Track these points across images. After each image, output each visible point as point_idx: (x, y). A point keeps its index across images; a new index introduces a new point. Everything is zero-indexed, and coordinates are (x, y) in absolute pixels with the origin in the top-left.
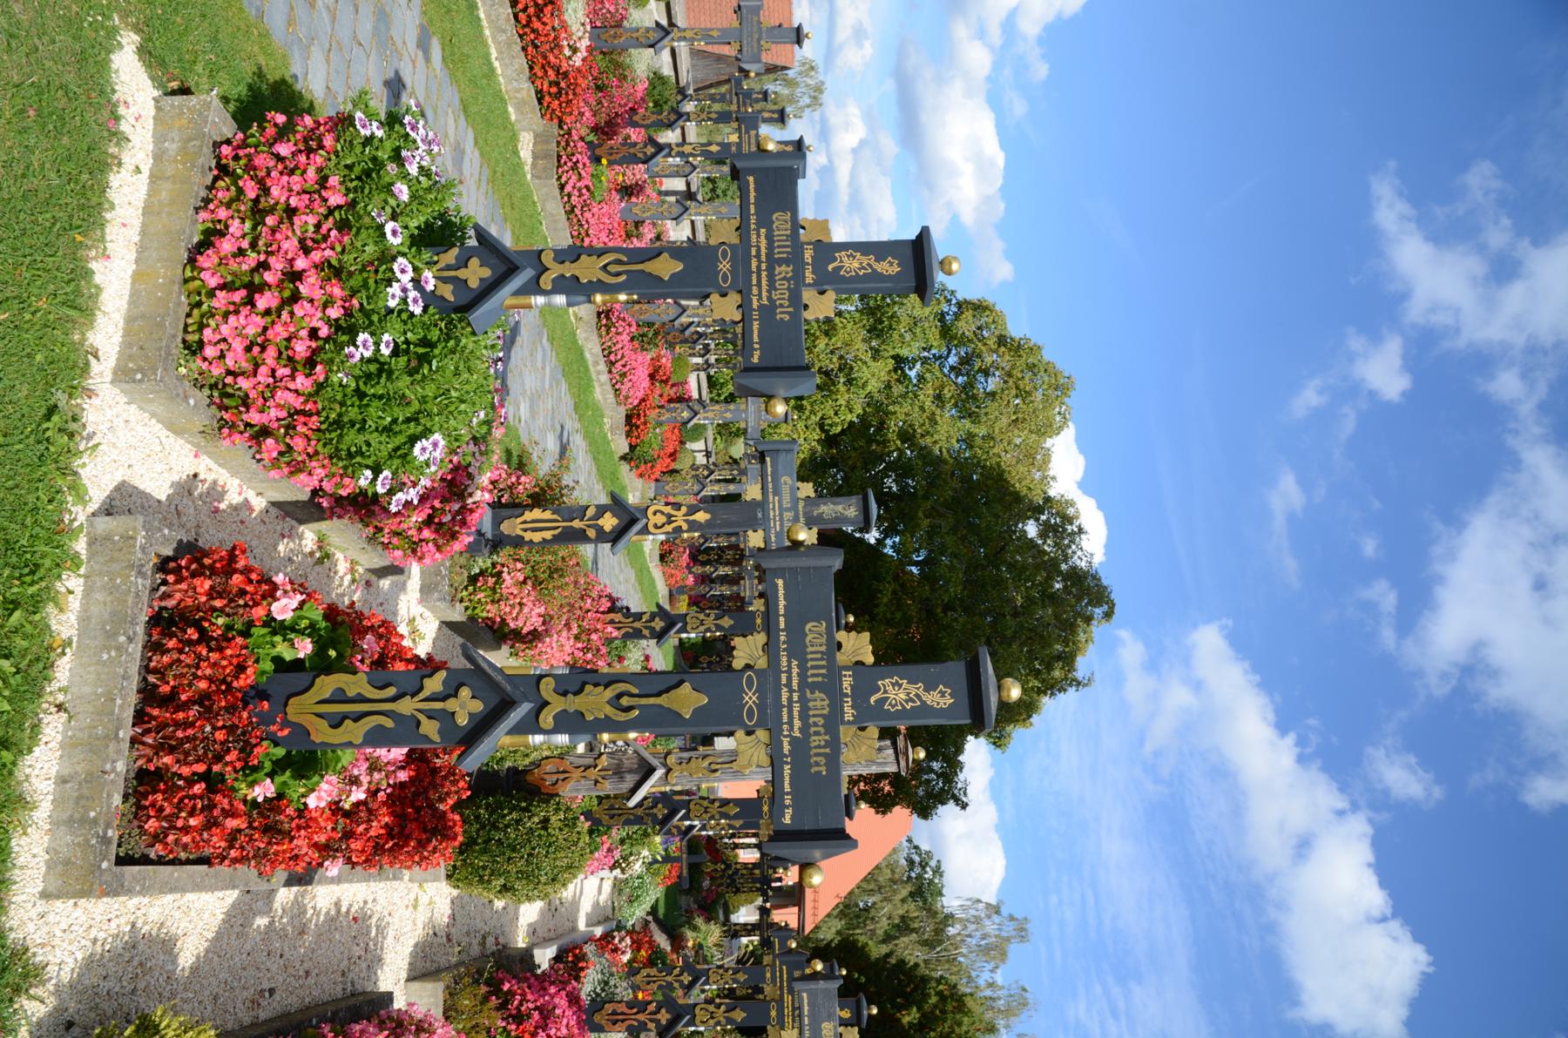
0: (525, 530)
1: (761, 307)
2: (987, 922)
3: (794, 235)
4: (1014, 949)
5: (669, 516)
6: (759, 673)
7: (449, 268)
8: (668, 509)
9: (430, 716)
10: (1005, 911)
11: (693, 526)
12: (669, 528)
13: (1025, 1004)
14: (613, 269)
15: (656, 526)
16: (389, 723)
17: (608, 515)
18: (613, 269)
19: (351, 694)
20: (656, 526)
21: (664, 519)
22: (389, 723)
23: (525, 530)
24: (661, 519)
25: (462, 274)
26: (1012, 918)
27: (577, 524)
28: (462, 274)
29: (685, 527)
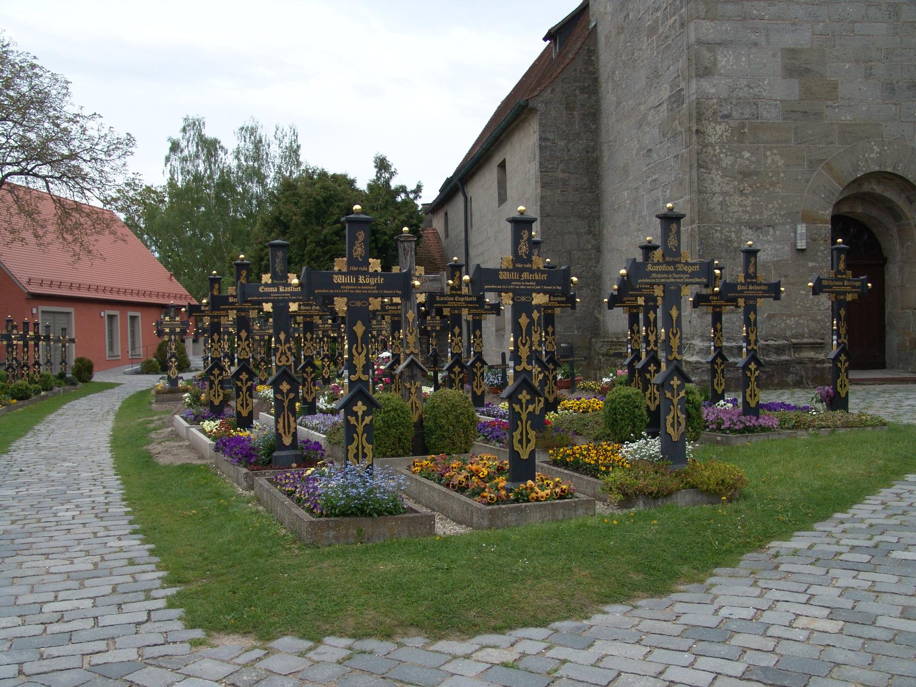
0: (289, 432)
1: (378, 289)
2: (186, 153)
3: (345, 274)
4: (209, 133)
5: (282, 354)
6: (515, 295)
7: (357, 420)
8: (278, 355)
9: (527, 408)
10: (178, 135)
11: (287, 341)
12: (289, 354)
13: (252, 131)
14: (360, 350)
15: (288, 361)
16: (529, 422)
17: (281, 387)
18: (360, 350)
19: (519, 437)
20: (288, 361)
21: (284, 357)
22: (529, 422)
23: (289, 432)
24: (284, 358)
25: (360, 414)
26: (184, 130)
27: (286, 404)
28: (360, 414)
29: (288, 345)
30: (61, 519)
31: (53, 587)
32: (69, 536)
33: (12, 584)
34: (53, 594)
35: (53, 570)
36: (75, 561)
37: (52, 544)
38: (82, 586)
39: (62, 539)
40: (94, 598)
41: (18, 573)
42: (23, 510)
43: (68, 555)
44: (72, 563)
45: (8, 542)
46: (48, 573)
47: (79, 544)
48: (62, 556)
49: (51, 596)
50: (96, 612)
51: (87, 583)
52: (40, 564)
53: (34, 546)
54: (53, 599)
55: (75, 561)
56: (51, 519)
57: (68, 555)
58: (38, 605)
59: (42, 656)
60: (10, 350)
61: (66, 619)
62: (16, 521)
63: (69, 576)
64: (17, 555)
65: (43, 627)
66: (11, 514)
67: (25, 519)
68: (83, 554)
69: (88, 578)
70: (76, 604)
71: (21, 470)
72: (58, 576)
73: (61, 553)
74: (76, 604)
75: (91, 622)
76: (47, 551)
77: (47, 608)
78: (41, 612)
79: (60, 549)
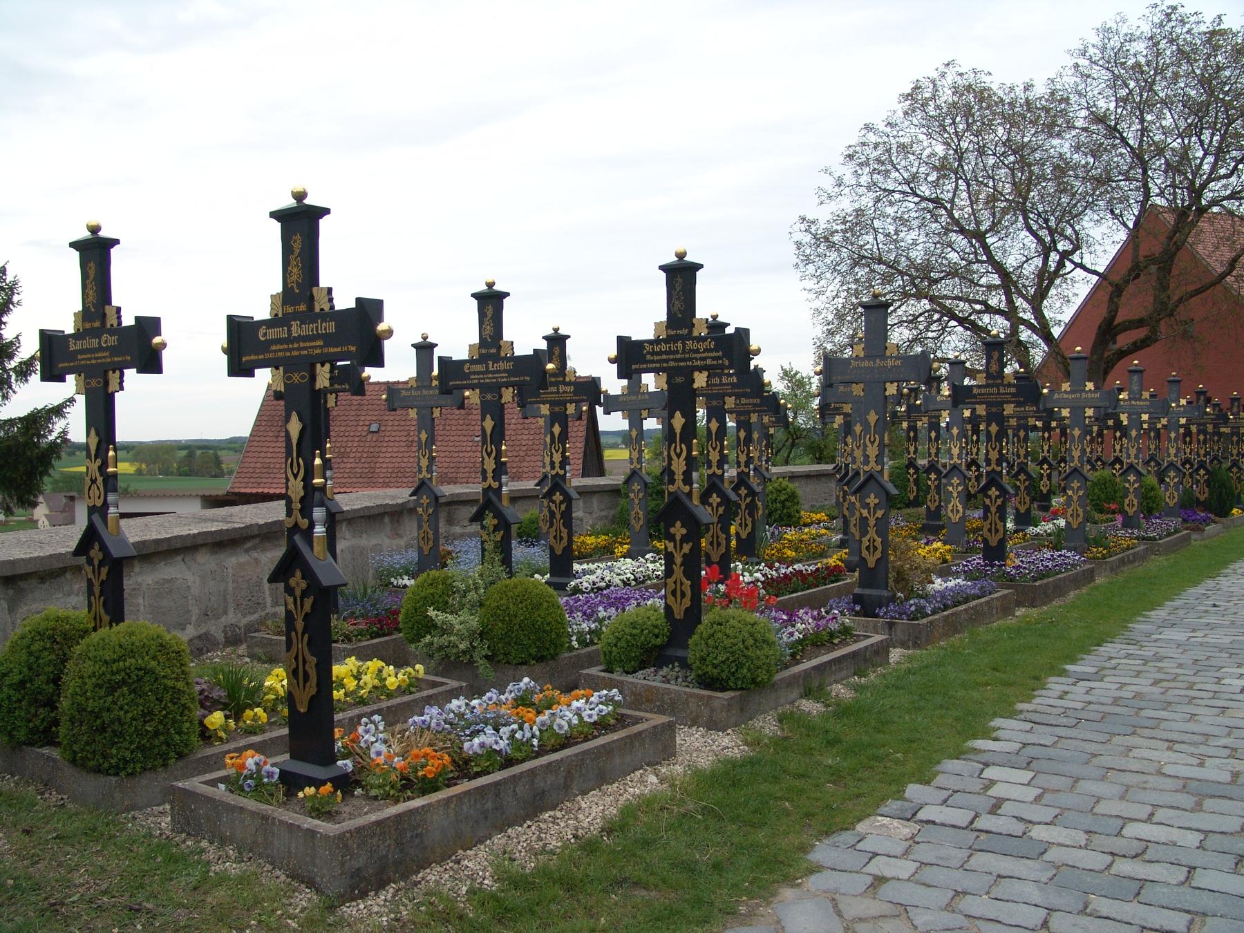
30: (1223, 689)
31: (1155, 798)
32: (1220, 720)
33: (1103, 778)
34: (1149, 809)
35: (1168, 770)
36: (1208, 762)
37: (1192, 727)
38: (1198, 807)
39: (1208, 721)
40: (1206, 832)
41: (1120, 763)
42: (1180, 666)
43: (1202, 749)
44: (1201, 765)
45: (1132, 712)
46: (1160, 773)
47: (1229, 735)
48: (1192, 749)
49: (1143, 812)
50: (1198, 859)
51: (1209, 804)
52: (1154, 755)
53: (1163, 725)
54: (1145, 816)
55: (1208, 762)
56: (1208, 687)
57: (1202, 749)
58: (1120, 822)
59: (1086, 907)
60: (1188, 439)
61: (1146, 857)
62: (1162, 680)
63: (1185, 784)
64: (1134, 733)
65: (1109, 858)
66: (1160, 670)
67: (1174, 680)
68: (1227, 752)
69: (1213, 797)
70: (1175, 835)
71: (1215, 606)
72: (1169, 780)
73: (1194, 744)
74: (1175, 835)
75: (1181, 874)
76: (1175, 736)
77: (1131, 830)
78: (1119, 834)
79: (1196, 738)
